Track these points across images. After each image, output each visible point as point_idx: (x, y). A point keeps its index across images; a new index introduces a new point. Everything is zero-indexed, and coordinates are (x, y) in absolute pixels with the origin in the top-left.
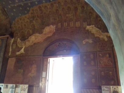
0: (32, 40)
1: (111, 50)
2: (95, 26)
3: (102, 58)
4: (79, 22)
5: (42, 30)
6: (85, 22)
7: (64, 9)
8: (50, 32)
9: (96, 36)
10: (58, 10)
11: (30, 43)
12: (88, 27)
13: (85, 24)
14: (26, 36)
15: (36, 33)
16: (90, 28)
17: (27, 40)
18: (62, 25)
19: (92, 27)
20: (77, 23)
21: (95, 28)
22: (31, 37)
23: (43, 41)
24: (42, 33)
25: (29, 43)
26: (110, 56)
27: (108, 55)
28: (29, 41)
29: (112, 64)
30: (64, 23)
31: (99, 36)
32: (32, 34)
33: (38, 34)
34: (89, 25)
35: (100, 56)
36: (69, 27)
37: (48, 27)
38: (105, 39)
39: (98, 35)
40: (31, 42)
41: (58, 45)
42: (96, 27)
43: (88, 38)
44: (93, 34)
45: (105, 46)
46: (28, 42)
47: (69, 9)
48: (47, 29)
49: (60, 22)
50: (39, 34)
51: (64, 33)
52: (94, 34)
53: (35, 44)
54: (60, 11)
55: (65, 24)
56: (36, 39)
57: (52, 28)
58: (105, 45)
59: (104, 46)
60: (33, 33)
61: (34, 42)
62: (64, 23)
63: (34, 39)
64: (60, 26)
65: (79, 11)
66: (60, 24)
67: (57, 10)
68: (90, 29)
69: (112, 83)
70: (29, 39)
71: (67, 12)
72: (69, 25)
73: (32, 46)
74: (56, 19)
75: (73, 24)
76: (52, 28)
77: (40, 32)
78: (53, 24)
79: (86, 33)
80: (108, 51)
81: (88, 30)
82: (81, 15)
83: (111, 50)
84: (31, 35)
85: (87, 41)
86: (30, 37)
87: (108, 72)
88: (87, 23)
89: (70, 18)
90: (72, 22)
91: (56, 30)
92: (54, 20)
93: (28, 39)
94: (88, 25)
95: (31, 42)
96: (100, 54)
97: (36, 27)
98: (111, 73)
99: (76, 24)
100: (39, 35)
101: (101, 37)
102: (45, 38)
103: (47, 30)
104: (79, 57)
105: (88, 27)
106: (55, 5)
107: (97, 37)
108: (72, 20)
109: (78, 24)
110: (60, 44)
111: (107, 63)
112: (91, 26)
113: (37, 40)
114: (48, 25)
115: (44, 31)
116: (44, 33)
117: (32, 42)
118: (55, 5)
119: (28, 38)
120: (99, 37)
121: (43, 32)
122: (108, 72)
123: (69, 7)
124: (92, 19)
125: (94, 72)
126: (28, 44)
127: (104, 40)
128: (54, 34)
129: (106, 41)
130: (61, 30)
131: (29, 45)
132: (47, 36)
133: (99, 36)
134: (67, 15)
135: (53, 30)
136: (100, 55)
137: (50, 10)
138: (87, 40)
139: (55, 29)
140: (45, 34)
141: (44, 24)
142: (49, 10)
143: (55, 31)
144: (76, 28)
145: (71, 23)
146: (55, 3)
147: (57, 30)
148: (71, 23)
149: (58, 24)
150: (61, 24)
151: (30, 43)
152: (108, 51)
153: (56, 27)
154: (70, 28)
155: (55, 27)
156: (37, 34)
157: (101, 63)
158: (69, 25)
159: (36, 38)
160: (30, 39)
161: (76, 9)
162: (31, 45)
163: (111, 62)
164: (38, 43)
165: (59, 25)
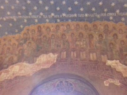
0: (13, 70)
2: (120, 62)
4: (95, 54)
5: (35, 58)
6: (103, 54)
7: (74, 34)
8: (48, 62)
10: (65, 35)
11: (8, 76)
12: (109, 62)
13: (104, 58)
14: (6, 64)
15: (23, 62)
16: (113, 63)
17: (5, 70)
18: (68, 55)
19: (116, 63)
20: (91, 54)
21: (121, 64)
22: (13, 67)
23: (33, 75)
24: (33, 62)
25: (7, 75)
28: (7, 72)
30: (72, 53)
32: (16, 63)
33: (26, 63)
34: (112, 59)
36: (79, 59)
37: (45, 56)
40: (11, 73)
41: (58, 86)
42: (122, 64)
43: (112, 78)
46: (6, 74)
47: (81, 36)
48: (43, 58)
49: (65, 51)
50: (29, 63)
51: (71, 66)
53: (16, 78)
54: (68, 37)
55: (73, 54)
56: (20, 70)
57: (53, 57)
60: (20, 60)
61: (17, 75)
62: (72, 53)
63: (17, 71)
64: (65, 56)
65: (94, 39)
66: (65, 53)
67: (63, 35)
68: (113, 65)
70: (9, 69)
71: (78, 39)
72: (79, 56)
73: (10, 80)
74: (60, 46)
75: (85, 55)
76: (53, 57)
77: (31, 60)
78: (54, 52)
79: (107, 70)
81: (110, 66)
82: (98, 45)
84: (13, 64)
85: (112, 82)
86: (10, 67)
88: (107, 56)
89: (82, 46)
90: (84, 52)
91: (57, 60)
92: (57, 46)
93: (7, 69)
94: (108, 60)
95: (11, 73)
97: (25, 54)
99: (90, 56)
100: (28, 64)
102: (38, 69)
103: (42, 59)
105: (109, 62)
106: (61, 27)
108: (84, 50)
109: (93, 56)
110: (61, 82)
112: (114, 61)
113: (23, 72)
114: (46, 52)
115: (38, 59)
116: (37, 62)
117: (13, 74)
118: (61, 27)
119: (7, 67)
121: (35, 61)
123: (80, 33)
124: (114, 52)
126: (5, 76)
128: (54, 65)
130: (66, 61)
131: (7, 78)
132: (42, 67)
134: (78, 43)
135: (52, 60)
137: (54, 33)
138: (111, 81)
139: (56, 59)
140: (38, 65)
141: (39, 51)
142: (51, 33)
143: (55, 61)
144: (90, 61)
145: (83, 55)
146: (62, 25)
147: (59, 60)
148: (83, 55)
149: (62, 53)
150: (67, 54)
151: (8, 76)
153: (58, 57)
154: (81, 60)
155: (56, 55)
156: (25, 64)
158: (79, 56)
159: (22, 69)
160: (10, 70)
161: (91, 36)
162: (9, 79)
164: (23, 76)
165: (63, 55)
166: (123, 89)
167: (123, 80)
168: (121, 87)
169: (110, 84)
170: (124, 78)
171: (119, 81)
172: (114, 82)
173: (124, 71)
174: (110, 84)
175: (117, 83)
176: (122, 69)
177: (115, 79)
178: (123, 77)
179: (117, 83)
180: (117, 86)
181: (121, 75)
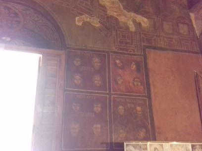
1: (141, 55)
3: (120, 71)
9: (109, 13)
26: (138, 69)
27: (134, 67)
29: (142, 87)
31: (118, 15)
35: (116, 64)
38: (130, 26)
39: (115, 13)
44: (103, 8)
45: (128, 43)
52: (106, 8)
58: (130, 41)
59: (126, 43)
69: (142, 134)
80: (134, 55)
83: (141, 55)
87: (133, 106)
96: (118, 59)
98: (139, 108)
101: (122, 19)
104: (63, 57)
107: (112, 17)
111: (131, 84)
120: (117, 19)
122: (133, 106)
125: (99, 105)
127: (128, 28)
129: (132, 32)
133: (118, 15)
136: (118, 62)
152: (134, 55)
157: (119, 82)
163: (139, 84)
166: (101, 32)
167: (105, 20)
168: (99, 29)
169: (85, 23)
170: (108, 17)
171: (98, 20)
172: (92, 20)
173: (111, 5)
174: (85, 23)
175: (96, 23)
176: (109, 2)
177: (94, 17)
178: (106, 15)
179: (96, 23)
180: (94, 27)
181: (104, 11)
